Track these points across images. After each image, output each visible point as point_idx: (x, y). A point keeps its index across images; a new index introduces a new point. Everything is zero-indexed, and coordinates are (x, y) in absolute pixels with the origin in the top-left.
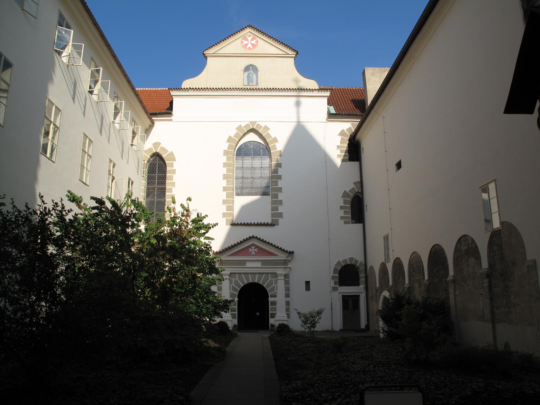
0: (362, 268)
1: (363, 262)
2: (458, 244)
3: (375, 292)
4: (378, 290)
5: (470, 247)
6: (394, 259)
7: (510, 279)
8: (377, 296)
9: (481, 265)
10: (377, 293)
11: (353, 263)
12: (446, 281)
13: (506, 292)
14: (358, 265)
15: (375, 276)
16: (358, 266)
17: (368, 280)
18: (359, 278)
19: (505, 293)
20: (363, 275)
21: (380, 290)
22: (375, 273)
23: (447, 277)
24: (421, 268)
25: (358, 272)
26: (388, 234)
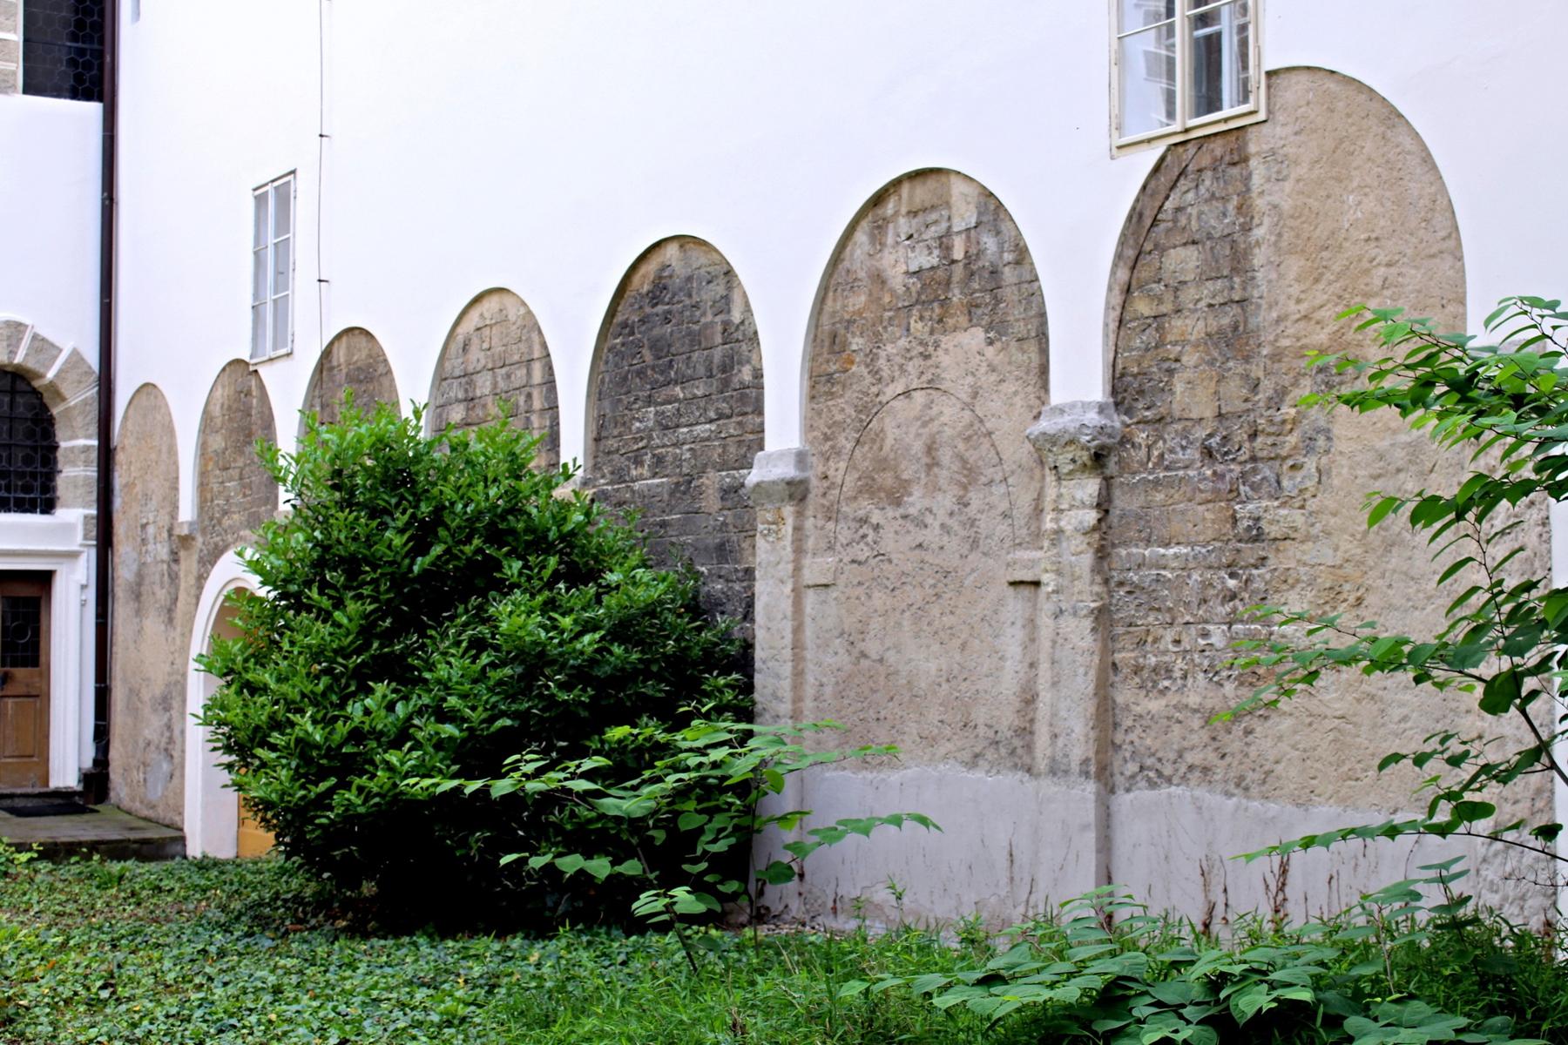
0: (78, 398)
1: (93, 358)
2: (861, 237)
3: (163, 552)
4: (186, 541)
5: (958, 254)
6: (325, 344)
7: (1285, 483)
8: (174, 578)
9: (1045, 385)
10: (176, 561)
11: (18, 359)
12: (732, 492)
13: (1232, 575)
14: (50, 375)
15: (172, 451)
16: (52, 384)
17: (119, 480)
18: (55, 461)
19: (1232, 583)
20: (81, 442)
21: (200, 539)
22: (169, 430)
23: (750, 466)
24: (529, 396)
25: (51, 421)
26: (293, 172)
